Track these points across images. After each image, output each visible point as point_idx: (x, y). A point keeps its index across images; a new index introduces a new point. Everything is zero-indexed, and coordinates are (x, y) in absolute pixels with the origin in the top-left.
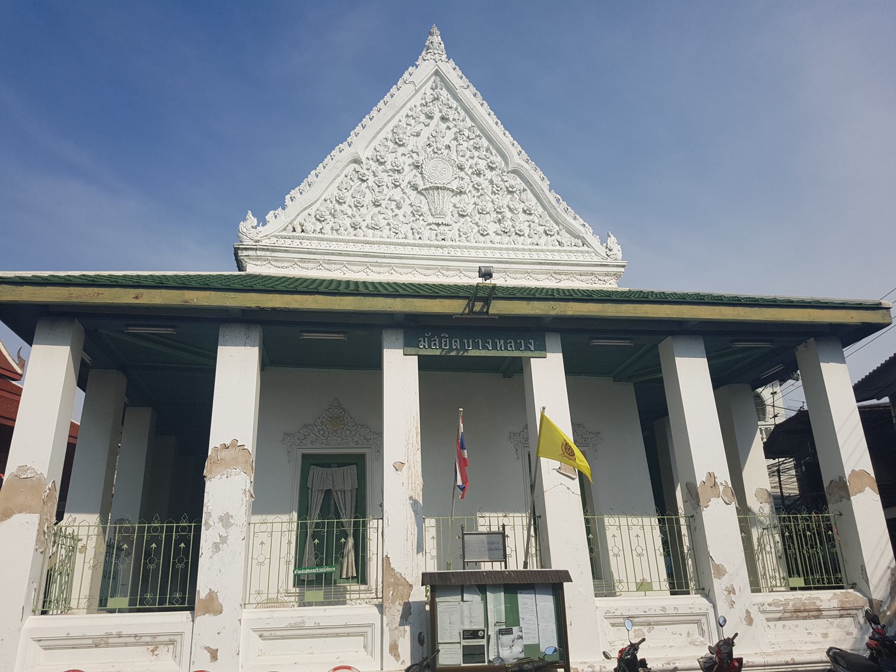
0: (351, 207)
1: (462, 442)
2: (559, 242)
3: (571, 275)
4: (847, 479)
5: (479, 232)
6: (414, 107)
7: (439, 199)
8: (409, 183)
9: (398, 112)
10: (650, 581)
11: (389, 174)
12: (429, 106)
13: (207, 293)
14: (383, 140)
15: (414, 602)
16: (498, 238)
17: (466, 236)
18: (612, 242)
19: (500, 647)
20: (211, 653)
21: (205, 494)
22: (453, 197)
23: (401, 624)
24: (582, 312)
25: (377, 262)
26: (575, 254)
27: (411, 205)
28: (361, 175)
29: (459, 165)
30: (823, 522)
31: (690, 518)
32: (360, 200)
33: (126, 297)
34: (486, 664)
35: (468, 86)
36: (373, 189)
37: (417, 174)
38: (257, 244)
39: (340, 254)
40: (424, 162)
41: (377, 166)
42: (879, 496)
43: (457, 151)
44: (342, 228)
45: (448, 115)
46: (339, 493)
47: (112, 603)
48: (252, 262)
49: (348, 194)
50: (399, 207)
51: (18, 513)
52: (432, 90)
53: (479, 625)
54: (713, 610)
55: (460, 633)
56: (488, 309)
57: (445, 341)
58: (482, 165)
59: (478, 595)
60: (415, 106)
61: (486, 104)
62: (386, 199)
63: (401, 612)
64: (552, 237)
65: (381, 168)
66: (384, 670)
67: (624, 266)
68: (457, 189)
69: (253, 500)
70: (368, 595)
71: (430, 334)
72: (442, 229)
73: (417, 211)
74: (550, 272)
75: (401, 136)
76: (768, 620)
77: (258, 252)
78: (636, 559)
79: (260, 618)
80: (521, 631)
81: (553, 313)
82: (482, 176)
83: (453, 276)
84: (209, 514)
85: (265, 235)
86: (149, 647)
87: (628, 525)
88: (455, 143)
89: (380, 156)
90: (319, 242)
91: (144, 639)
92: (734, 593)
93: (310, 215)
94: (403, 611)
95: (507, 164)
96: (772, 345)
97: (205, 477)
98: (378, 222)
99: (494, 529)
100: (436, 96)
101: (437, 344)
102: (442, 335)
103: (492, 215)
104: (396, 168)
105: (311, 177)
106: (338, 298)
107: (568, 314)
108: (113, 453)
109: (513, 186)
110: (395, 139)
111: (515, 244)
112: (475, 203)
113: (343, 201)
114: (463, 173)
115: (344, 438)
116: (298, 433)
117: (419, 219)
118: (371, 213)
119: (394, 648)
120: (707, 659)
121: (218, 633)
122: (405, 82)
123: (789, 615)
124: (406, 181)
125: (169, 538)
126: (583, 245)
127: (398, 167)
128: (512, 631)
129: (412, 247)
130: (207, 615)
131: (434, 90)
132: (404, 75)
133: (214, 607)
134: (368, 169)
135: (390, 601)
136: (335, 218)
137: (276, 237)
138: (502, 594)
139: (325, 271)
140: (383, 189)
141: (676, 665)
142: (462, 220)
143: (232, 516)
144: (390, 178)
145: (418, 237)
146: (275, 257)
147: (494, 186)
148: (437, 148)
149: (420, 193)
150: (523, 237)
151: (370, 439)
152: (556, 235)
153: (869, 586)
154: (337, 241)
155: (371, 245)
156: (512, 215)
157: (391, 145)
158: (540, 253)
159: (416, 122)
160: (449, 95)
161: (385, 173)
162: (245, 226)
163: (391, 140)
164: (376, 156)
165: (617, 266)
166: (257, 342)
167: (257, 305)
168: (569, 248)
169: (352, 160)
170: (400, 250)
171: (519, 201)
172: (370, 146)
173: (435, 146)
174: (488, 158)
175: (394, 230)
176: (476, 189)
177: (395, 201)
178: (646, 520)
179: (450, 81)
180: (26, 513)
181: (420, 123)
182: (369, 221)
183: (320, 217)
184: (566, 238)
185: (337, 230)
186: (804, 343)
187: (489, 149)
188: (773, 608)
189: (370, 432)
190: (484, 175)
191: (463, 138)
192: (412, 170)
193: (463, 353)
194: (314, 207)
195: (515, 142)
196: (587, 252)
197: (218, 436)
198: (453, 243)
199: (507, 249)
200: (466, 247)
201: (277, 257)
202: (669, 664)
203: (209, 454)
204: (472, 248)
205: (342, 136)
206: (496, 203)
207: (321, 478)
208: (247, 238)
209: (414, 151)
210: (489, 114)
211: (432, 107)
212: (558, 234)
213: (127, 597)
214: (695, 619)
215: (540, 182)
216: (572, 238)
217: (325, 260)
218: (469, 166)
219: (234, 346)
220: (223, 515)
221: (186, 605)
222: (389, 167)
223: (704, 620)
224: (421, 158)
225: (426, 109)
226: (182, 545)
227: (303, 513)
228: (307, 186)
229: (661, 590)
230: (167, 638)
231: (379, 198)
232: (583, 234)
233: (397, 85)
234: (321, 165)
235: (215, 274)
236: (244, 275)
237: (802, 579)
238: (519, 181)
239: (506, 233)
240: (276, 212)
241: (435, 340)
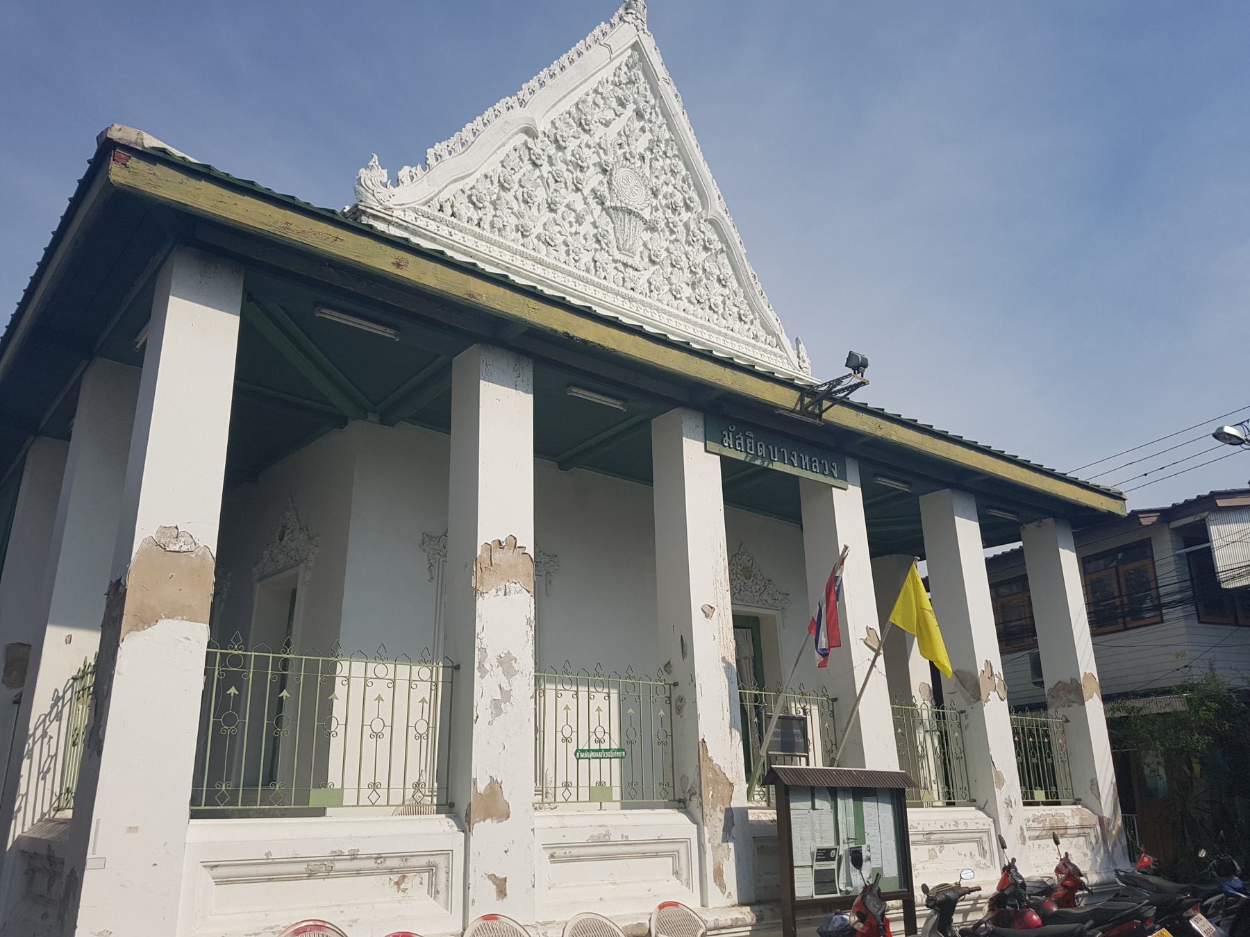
0: (517, 199)
5: (670, 290)
13: (502, 290)
14: (564, 114)
15: (736, 808)
16: (691, 308)
23: (725, 840)
24: (903, 439)
27: (594, 225)
29: (654, 189)
34: (839, 895)
54: (993, 825)
55: (812, 854)
58: (678, 198)
59: (828, 801)
63: (723, 822)
71: (734, 427)
77: (391, 227)
80: (869, 851)
81: (879, 433)
85: (401, 203)
86: (392, 876)
88: (648, 155)
89: (562, 136)
91: (391, 863)
93: (463, 192)
94: (725, 821)
96: (1018, 518)
100: (633, 78)
102: (747, 434)
104: (579, 162)
109: (711, 241)
113: (508, 187)
119: (718, 874)
121: (506, 852)
127: (582, 162)
129: (595, 288)
130: (489, 821)
132: (595, 30)
135: (710, 806)
137: (415, 211)
145: (603, 275)
148: (631, 153)
149: (605, 210)
153: (1100, 802)
155: (544, 268)
158: (735, 342)
166: (531, 388)
167: (565, 330)
169: (524, 128)
177: (574, 211)
180: (183, 619)
181: (610, 108)
182: (539, 229)
183: (478, 200)
184: (757, 328)
190: (679, 214)
192: (597, 174)
193: (768, 464)
196: (781, 357)
197: (487, 532)
206: (691, 259)
208: (373, 198)
219: (501, 385)
222: (569, 158)
225: (620, 93)
230: (423, 861)
237: (1043, 791)
240: (413, 170)
241: (740, 439)
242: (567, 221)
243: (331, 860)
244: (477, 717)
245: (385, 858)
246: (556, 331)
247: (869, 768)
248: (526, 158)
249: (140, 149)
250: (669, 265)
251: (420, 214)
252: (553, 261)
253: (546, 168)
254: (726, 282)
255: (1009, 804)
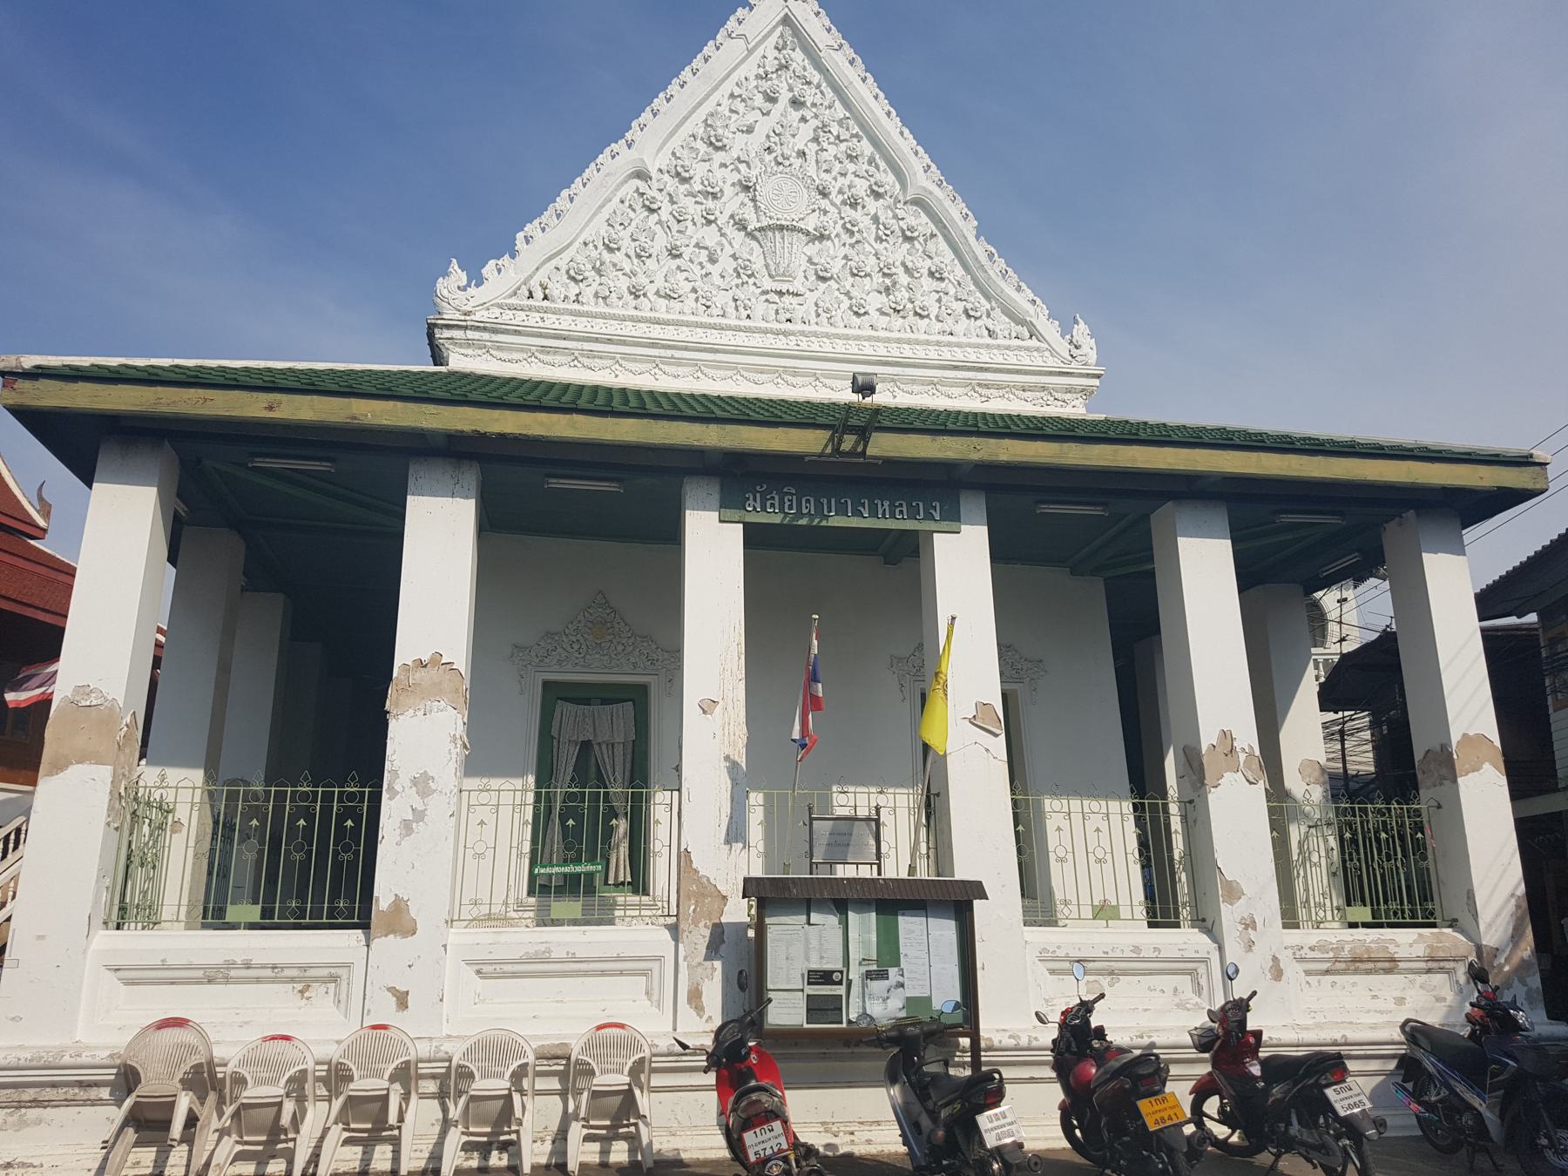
0: (629, 257)
1: (814, 670)
2: (989, 331)
3: (1008, 389)
4: (1454, 748)
5: (850, 308)
6: (744, 80)
7: (783, 248)
8: (732, 217)
9: (716, 88)
10: (1116, 904)
11: (697, 199)
12: (771, 79)
13: (391, 404)
17: (829, 316)
18: (1080, 332)
19: (867, 999)
20: (397, 998)
21: (388, 741)
22: (807, 244)
23: (707, 958)
24: (1025, 456)
25: (672, 357)
26: (1016, 352)
27: (734, 257)
28: (647, 199)
29: (821, 187)
30: (1409, 817)
31: (1187, 804)
32: (646, 245)
33: (252, 406)
34: (844, 1025)
35: (841, 46)
36: (668, 227)
37: (746, 201)
38: (467, 318)
39: (610, 341)
40: (760, 181)
41: (677, 184)
42: (1505, 777)
43: (817, 162)
44: (613, 295)
45: (804, 97)
46: (604, 747)
47: (233, 913)
48: (458, 349)
49: (625, 234)
50: (713, 261)
51: (77, 763)
52: (776, 51)
53: (834, 964)
54: (1217, 953)
55: (803, 975)
56: (865, 447)
57: (789, 501)
58: (861, 188)
59: (836, 916)
60: (746, 79)
61: (870, 80)
62: (691, 246)
63: (707, 939)
64: (978, 321)
65: (683, 188)
66: (678, 1030)
67: (1098, 376)
68: (815, 230)
69: (467, 753)
70: (654, 912)
72: (787, 301)
73: (745, 268)
74: (971, 384)
75: (720, 131)
76: (1308, 973)
78: (1095, 867)
79: (478, 944)
80: (902, 975)
81: (975, 456)
82: (859, 207)
83: (803, 386)
84: (395, 773)
86: (295, 985)
87: (1083, 812)
88: (814, 147)
89: (682, 166)
90: (574, 318)
91: (288, 973)
92: (1255, 929)
95: (904, 187)
96: (1343, 521)
97: (388, 712)
98: (675, 286)
99: (863, 812)
100: (783, 61)
101: (777, 505)
102: (785, 490)
103: (874, 279)
104: (709, 189)
105: (561, 202)
106: (610, 421)
107: (1001, 459)
108: (224, 669)
109: (913, 227)
110: (709, 137)
111: (912, 332)
112: (846, 257)
113: (616, 246)
114: (827, 201)
115: (614, 656)
116: (537, 646)
117: (747, 283)
118: (665, 270)
119: (695, 996)
120: (1204, 1031)
121: (410, 966)
122: (729, 36)
123: (1343, 966)
124: (727, 213)
125: (326, 811)
126: (1031, 336)
127: (713, 188)
128: (887, 974)
129: (735, 333)
130: (391, 936)
131: (780, 50)
132: (728, 22)
133: (402, 923)
134: (661, 190)
135: (690, 921)
136: (601, 276)
137: (500, 306)
138: (874, 914)
139: (583, 369)
140: (687, 227)
141: (1152, 1039)
142: (822, 286)
143: (433, 778)
144: (699, 207)
145: (745, 314)
146: (497, 342)
147: (881, 226)
148: (782, 155)
149: (750, 235)
150: (926, 320)
151: (657, 660)
152: (984, 317)
154: (604, 316)
155: (663, 327)
156: (909, 279)
157: (703, 148)
158: (955, 349)
159: (746, 106)
160: (806, 61)
161: (690, 198)
162: (446, 285)
163: (702, 139)
164: (676, 166)
165: (1088, 375)
166: (473, 492)
167: (474, 428)
168: (1007, 342)
169: (632, 173)
170: (713, 337)
171: (922, 255)
172: (665, 148)
173: (779, 152)
174: (872, 176)
175: (704, 301)
176: (848, 230)
177: (706, 248)
178: (1114, 805)
179: (809, 36)
181: (753, 109)
182: (660, 283)
183: (576, 273)
184: (1001, 323)
185: (604, 298)
186: (1397, 519)
187: (875, 159)
188: (1317, 954)
189: (657, 648)
190: (864, 207)
191: (828, 139)
192: (737, 194)
194: (566, 256)
195: (920, 149)
196: (1037, 350)
197: (406, 650)
198: (806, 328)
199: (898, 341)
200: (827, 336)
201: (501, 342)
202: (1142, 1038)
203: (395, 674)
204: (837, 336)
205: (617, 131)
206: (882, 258)
207: (575, 721)
208: (449, 306)
209: (742, 159)
210: (876, 97)
211: (776, 82)
212: (988, 315)
213: (258, 904)
214: (1188, 968)
215: (961, 222)
216: (1013, 324)
217: (583, 350)
218: (837, 189)
219: (434, 496)
220: (418, 775)
221: (356, 920)
222: (698, 187)
223: (1202, 969)
224: (754, 172)
225: (765, 85)
226: (349, 823)
227: (545, 777)
228: (554, 217)
229: (1133, 919)
230: (325, 972)
231: (678, 243)
232: (1032, 317)
233: (715, 39)
234: (578, 180)
235: (396, 370)
236: (444, 373)
237: (1369, 909)
238: (924, 218)
239: (899, 311)
240: (500, 262)
241: (773, 498)
242: (696, 263)
243: (228, 968)
244: (383, 837)
245: (282, 968)
246: (462, 432)
247: (958, 876)
248: (638, 207)
249: (21, 371)
250: (849, 275)
251: (506, 308)
252: (677, 317)
253: (666, 208)
254: (941, 274)
255: (1250, 924)
